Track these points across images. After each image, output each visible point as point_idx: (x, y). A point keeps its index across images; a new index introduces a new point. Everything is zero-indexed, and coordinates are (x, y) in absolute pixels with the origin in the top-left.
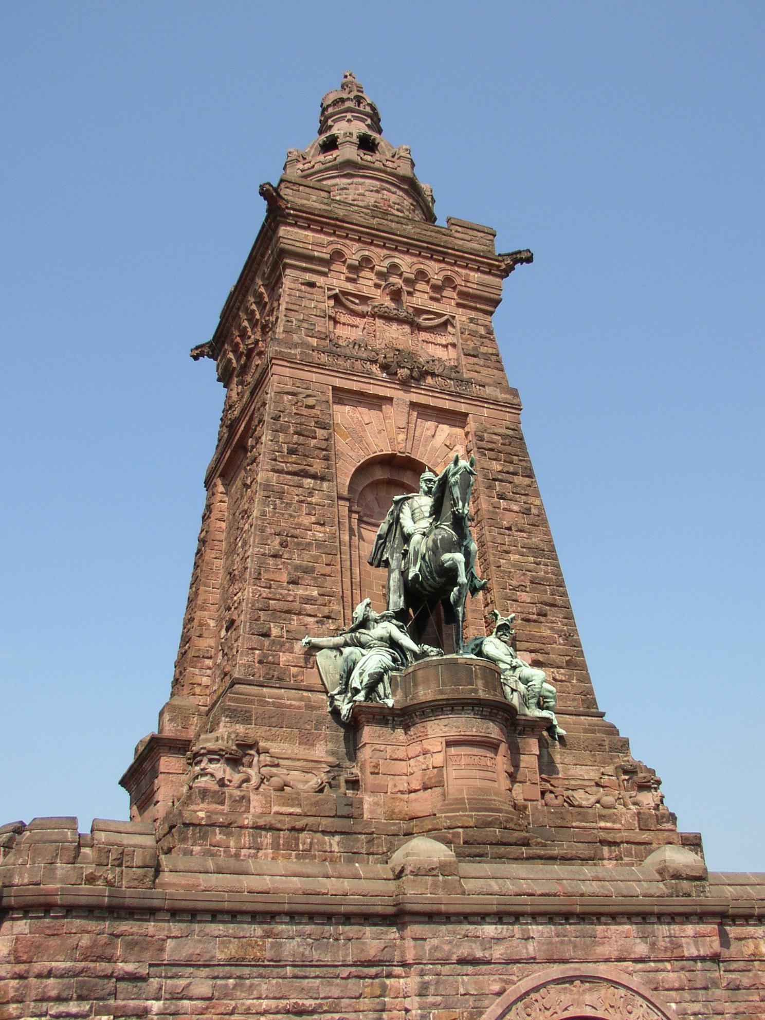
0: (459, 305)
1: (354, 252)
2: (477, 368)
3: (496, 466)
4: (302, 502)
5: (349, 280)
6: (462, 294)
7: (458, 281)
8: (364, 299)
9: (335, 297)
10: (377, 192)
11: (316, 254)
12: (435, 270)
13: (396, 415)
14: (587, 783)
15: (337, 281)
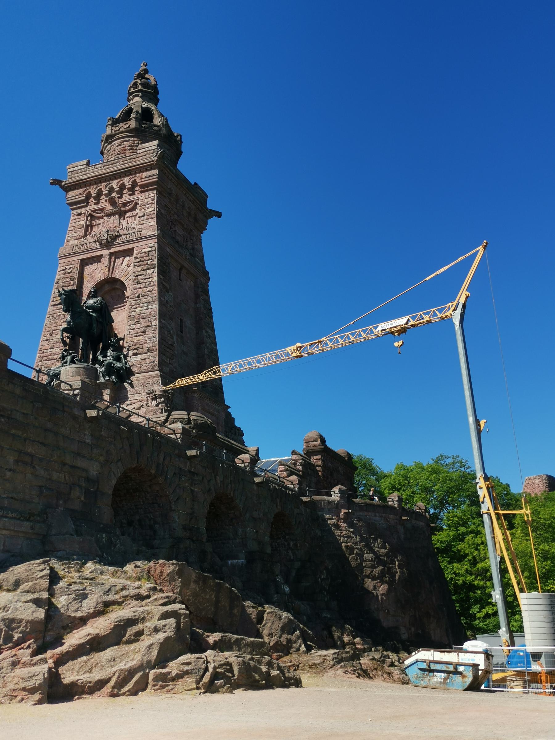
0: (141, 192)
1: (93, 191)
2: (142, 222)
3: (139, 268)
4: (60, 315)
5: (96, 204)
6: (142, 186)
7: (138, 180)
8: (102, 210)
9: (91, 215)
10: (120, 145)
11: (80, 199)
12: (127, 181)
13: (105, 261)
14: (137, 401)
15: (92, 206)
